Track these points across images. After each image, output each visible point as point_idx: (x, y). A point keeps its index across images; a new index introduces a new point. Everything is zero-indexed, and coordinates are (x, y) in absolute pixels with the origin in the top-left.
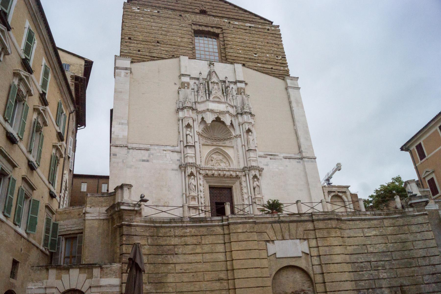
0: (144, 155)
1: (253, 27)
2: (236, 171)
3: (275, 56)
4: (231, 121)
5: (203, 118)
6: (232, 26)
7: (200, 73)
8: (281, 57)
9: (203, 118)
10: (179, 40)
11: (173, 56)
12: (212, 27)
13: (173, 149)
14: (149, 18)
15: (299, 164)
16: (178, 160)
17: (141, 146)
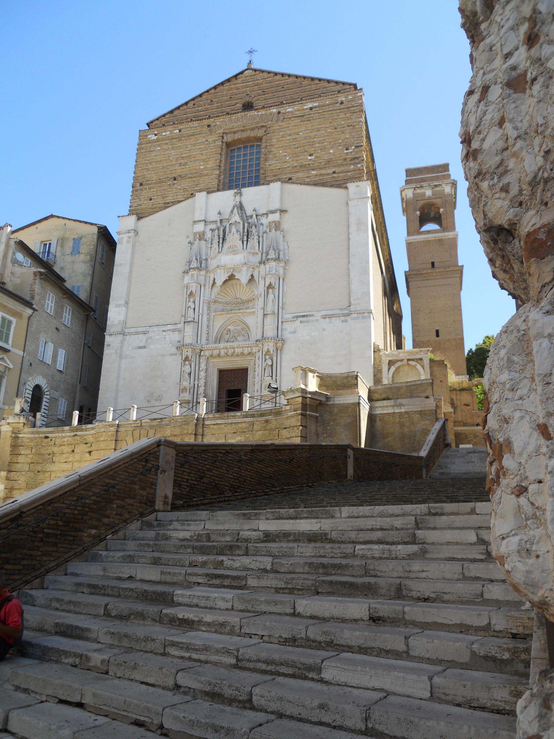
0: (141, 340)
1: (315, 107)
2: (248, 347)
3: (344, 149)
4: (252, 276)
5: (214, 279)
6: (282, 118)
7: (219, 213)
8: (353, 147)
9: (214, 279)
10: (201, 167)
11: (192, 194)
12: (252, 129)
13: (174, 328)
14: (167, 144)
15: (345, 324)
16: (179, 342)
17: (140, 330)
